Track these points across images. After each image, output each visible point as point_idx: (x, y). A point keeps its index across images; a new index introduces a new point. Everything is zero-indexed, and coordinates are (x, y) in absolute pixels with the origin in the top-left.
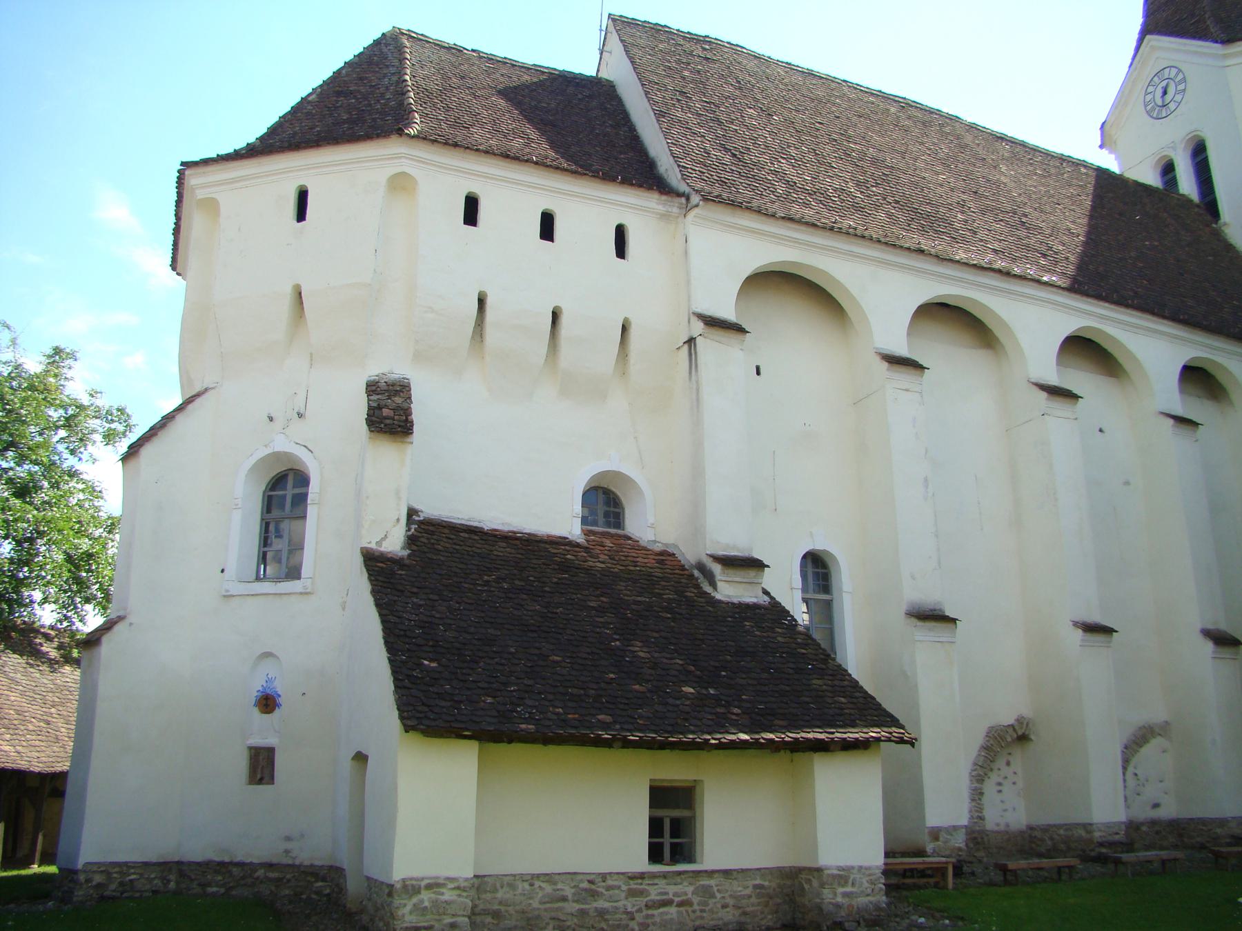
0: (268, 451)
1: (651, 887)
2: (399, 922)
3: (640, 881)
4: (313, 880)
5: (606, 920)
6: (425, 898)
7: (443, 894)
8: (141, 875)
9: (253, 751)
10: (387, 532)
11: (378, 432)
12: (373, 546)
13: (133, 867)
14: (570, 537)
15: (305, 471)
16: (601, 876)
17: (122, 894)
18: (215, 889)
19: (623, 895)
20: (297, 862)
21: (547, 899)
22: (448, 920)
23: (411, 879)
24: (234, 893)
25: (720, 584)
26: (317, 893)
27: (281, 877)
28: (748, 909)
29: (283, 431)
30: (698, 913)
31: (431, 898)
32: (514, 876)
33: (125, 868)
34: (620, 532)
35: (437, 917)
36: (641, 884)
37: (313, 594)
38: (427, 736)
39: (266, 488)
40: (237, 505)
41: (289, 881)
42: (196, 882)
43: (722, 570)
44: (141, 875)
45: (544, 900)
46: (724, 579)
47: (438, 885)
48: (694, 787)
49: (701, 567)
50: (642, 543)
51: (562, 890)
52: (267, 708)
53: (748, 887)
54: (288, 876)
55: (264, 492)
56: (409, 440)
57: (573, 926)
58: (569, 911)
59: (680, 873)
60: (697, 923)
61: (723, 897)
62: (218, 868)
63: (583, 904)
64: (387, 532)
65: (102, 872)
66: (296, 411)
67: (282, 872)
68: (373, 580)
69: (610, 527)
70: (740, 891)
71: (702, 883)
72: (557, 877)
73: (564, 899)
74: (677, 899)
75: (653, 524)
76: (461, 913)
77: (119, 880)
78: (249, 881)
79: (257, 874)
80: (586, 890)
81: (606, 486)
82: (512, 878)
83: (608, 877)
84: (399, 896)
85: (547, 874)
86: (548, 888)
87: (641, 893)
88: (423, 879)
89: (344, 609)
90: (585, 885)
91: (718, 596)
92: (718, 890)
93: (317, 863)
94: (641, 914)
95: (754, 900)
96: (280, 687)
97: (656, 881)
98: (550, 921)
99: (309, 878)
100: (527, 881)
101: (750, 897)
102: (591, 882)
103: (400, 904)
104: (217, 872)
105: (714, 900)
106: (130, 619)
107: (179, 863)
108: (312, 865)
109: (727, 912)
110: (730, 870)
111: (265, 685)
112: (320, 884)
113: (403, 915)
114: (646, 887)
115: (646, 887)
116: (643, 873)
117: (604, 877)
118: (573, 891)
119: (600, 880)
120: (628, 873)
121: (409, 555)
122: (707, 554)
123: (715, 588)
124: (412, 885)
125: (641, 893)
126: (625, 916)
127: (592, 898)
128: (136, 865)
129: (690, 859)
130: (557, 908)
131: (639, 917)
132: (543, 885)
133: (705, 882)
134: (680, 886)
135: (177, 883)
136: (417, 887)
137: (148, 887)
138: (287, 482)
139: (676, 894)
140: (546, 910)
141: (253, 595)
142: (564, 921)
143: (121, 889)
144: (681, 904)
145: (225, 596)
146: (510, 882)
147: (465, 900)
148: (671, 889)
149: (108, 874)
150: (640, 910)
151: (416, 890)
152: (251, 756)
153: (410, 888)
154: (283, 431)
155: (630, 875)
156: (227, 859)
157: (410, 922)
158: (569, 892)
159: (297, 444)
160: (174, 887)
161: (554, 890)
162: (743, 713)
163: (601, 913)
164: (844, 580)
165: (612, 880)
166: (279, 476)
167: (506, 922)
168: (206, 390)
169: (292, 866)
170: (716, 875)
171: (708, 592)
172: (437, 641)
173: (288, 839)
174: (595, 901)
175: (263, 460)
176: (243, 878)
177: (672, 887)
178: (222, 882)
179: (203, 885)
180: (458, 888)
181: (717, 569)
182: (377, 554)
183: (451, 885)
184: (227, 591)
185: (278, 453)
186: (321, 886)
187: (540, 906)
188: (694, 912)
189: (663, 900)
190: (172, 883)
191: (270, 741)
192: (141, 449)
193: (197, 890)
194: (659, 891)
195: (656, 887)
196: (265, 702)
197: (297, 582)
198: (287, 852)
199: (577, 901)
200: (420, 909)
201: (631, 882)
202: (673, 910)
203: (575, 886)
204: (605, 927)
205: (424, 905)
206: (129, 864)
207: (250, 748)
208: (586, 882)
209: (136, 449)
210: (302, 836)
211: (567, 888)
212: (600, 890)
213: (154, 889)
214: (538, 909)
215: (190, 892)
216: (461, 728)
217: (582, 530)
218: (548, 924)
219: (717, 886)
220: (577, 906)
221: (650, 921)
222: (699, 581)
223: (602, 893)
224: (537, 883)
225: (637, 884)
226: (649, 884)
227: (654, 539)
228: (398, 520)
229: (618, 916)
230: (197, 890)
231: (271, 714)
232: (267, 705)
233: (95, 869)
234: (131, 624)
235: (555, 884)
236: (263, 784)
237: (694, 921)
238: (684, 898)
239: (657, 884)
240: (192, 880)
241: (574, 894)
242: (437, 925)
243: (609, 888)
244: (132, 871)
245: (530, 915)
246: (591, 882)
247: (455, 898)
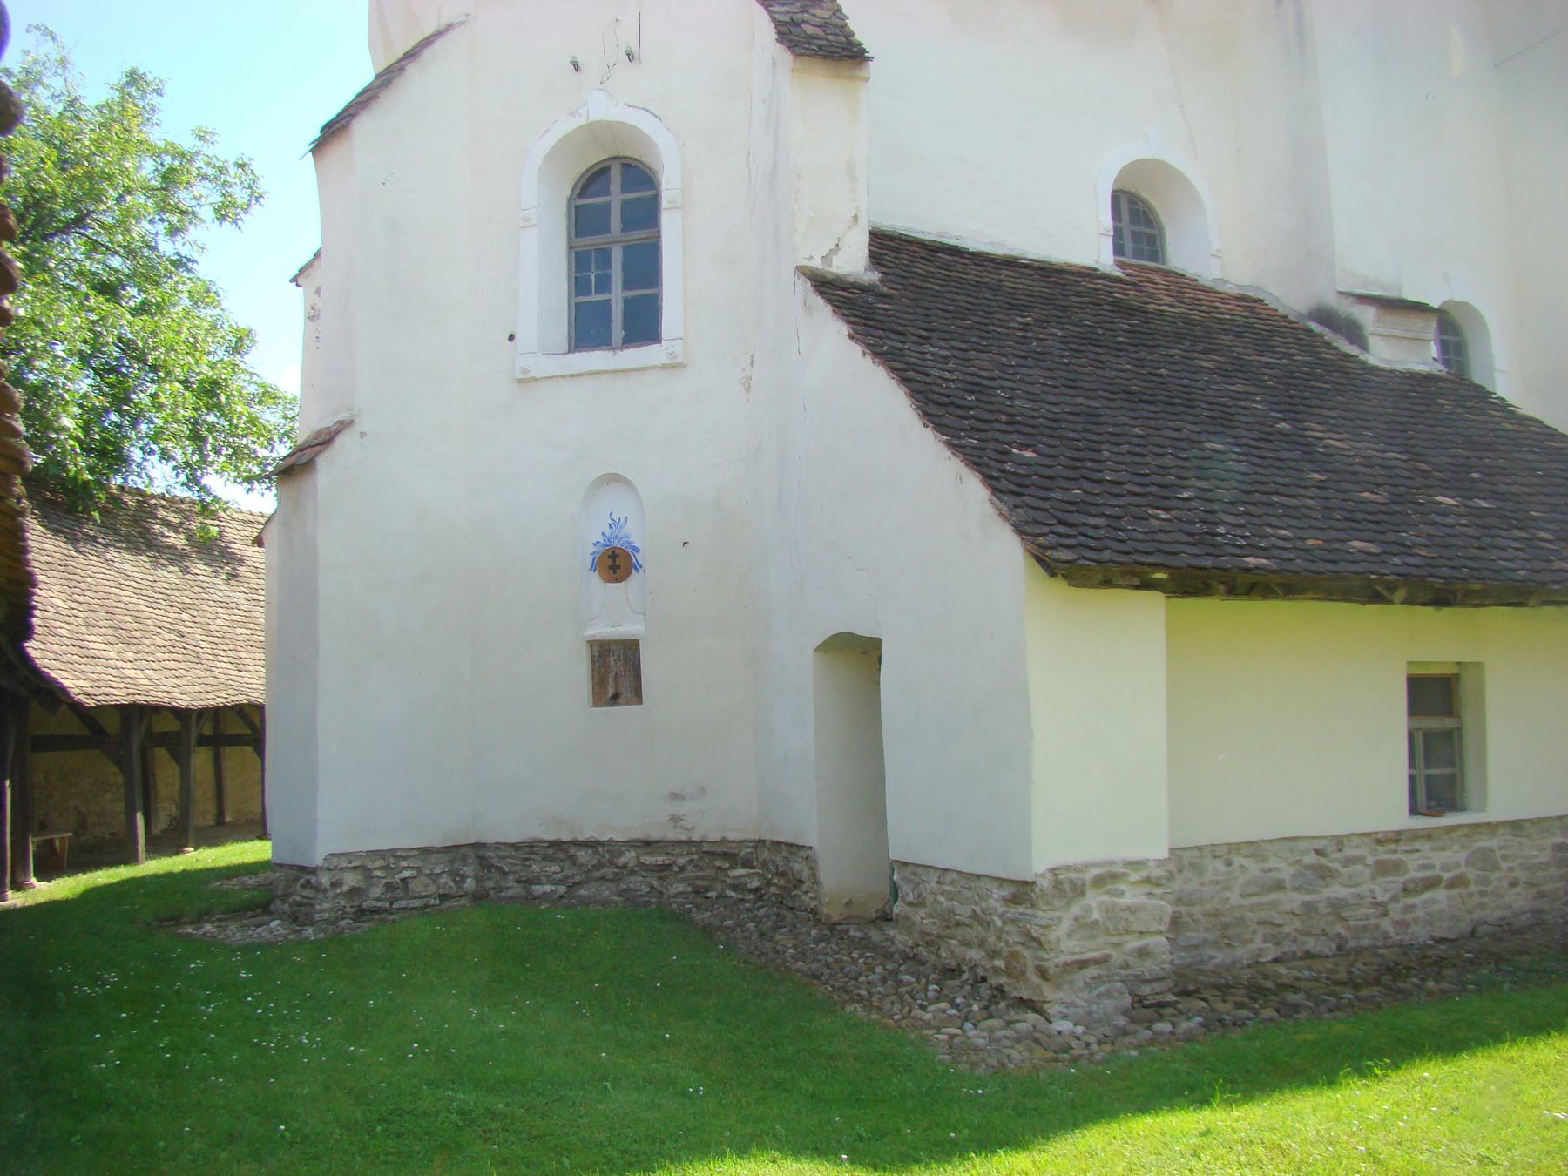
0: (581, 121)
1: (1410, 855)
2: (1052, 955)
3: (1392, 847)
4: (728, 865)
5: (1343, 919)
6: (1093, 905)
7: (1122, 893)
8: (419, 869)
9: (596, 648)
10: (839, 239)
11: (810, 56)
12: (817, 264)
13: (405, 858)
14: (1100, 268)
15: (643, 159)
16: (1335, 841)
17: (391, 903)
18: (548, 888)
19: (1368, 872)
20: (696, 837)
21: (1252, 889)
22: (1133, 943)
23: (1068, 868)
24: (582, 892)
25: (1373, 342)
26: (734, 887)
27: (667, 862)
28: (1548, 887)
29: (601, 87)
30: (1477, 899)
31: (1103, 902)
32: (1200, 848)
33: (392, 860)
34: (1161, 266)
35: (1115, 939)
36: (1395, 851)
37: (685, 366)
38: (1076, 586)
39: (572, 194)
40: (527, 220)
41: (682, 869)
42: (511, 878)
43: (1376, 315)
44: (419, 869)
45: (1248, 891)
46: (1380, 331)
47: (1114, 877)
48: (1457, 677)
49: (1326, 317)
50: (1202, 282)
51: (1277, 869)
52: (615, 572)
53: (1545, 849)
54: (681, 861)
55: (569, 200)
56: (863, 74)
57: (1294, 934)
58: (1288, 907)
59: (1450, 829)
60: (1477, 915)
61: (1511, 869)
62: (551, 851)
63: (1309, 892)
64: (839, 239)
65: (355, 868)
66: (623, 49)
67: (667, 854)
68: (847, 316)
69: (1143, 259)
70: (1536, 856)
71: (1478, 844)
72: (1267, 846)
73: (1279, 886)
74: (1446, 876)
75: (1219, 251)
76: (1154, 927)
77: (385, 880)
78: (609, 871)
79: (622, 860)
80: (1311, 867)
81: (1133, 190)
82: (1196, 853)
83: (1346, 842)
84: (1048, 904)
85: (1251, 843)
86: (1254, 868)
87: (1397, 867)
88: (1087, 866)
89: (748, 389)
90: (1310, 859)
91: (1372, 361)
92: (1504, 857)
93: (732, 836)
94: (1398, 906)
95: (1553, 871)
96: (634, 534)
97: (1417, 845)
98: (1259, 928)
99: (718, 863)
100: (1220, 857)
101: (1548, 864)
102: (1319, 853)
103: (1051, 919)
104: (546, 858)
105: (1497, 874)
106: (363, 424)
107: (478, 846)
108: (724, 841)
109: (1518, 894)
110: (1523, 820)
111: (608, 532)
112: (740, 871)
113: (1058, 941)
114: (1403, 857)
115: (1403, 857)
116: (1399, 833)
117: (1340, 841)
118: (1291, 870)
119: (1335, 848)
120: (1377, 833)
121: (881, 281)
122: (1341, 293)
123: (1363, 345)
124: (1071, 881)
125: (1397, 867)
126: (1373, 910)
127: (1321, 882)
128: (411, 854)
129: (1455, 806)
130: (1270, 904)
131: (1395, 911)
132: (1246, 862)
133: (1485, 842)
134: (1448, 853)
135: (478, 879)
136: (1080, 883)
137: (432, 889)
138: (608, 181)
139: (1445, 868)
140: (1251, 908)
141: (572, 376)
142: (1279, 926)
143: (389, 895)
144: (1452, 884)
145: (520, 381)
146: (1192, 861)
147: (1162, 903)
148: (1439, 858)
149: (366, 870)
150: (1394, 899)
151: (1079, 891)
152: (593, 657)
153: (1067, 886)
154: (601, 87)
155: (1380, 836)
156: (566, 837)
157: (1071, 953)
158: (1286, 872)
159: (630, 106)
160: (474, 886)
161: (1264, 871)
162: (1557, 539)
163: (1337, 906)
164: (1495, 351)
165: (1352, 847)
166: (596, 169)
167: (1190, 934)
168: (450, 27)
169: (690, 843)
170: (1501, 830)
171: (1353, 354)
172: (1012, 415)
173: (676, 796)
174: (1327, 886)
175: (566, 140)
176: (595, 868)
177: (1439, 853)
178: (559, 876)
179: (527, 882)
180: (1147, 880)
181: (1367, 316)
182: (829, 277)
183: (1134, 877)
184: (525, 371)
185: (599, 123)
186: (742, 876)
187: (1244, 902)
188: (1470, 896)
189: (1427, 879)
190: (469, 880)
191: (628, 628)
192: (353, 122)
193: (518, 890)
194: (1421, 862)
195: (1417, 855)
196: (610, 562)
197: (655, 347)
198: (675, 819)
199: (1297, 889)
200: (1084, 925)
201: (1380, 848)
202: (1440, 894)
203: (1298, 862)
204: (1343, 932)
205: (1091, 919)
206: (399, 853)
207: (591, 644)
208: (1313, 854)
209: (344, 122)
210: (703, 790)
211: (1282, 866)
212: (1334, 865)
213: (441, 891)
214: (1240, 906)
215: (503, 894)
216: (1150, 565)
217: (1115, 261)
218: (1254, 932)
219: (1501, 848)
220: (1301, 897)
221: (1408, 917)
222: (1326, 338)
223: (1337, 871)
224: (1238, 860)
225: (1388, 852)
226: (1407, 851)
227: (1220, 276)
228: (855, 218)
229: (1363, 911)
230: (518, 890)
232: (614, 568)
233: (344, 864)
234: (363, 434)
235: (1265, 860)
236: (619, 705)
237: (1470, 912)
238: (1457, 872)
239: (1418, 851)
240: (504, 873)
241: (1294, 876)
242: (1113, 952)
243: (1349, 861)
244: (405, 864)
245: (1226, 919)
246: (1319, 853)
247: (1143, 899)
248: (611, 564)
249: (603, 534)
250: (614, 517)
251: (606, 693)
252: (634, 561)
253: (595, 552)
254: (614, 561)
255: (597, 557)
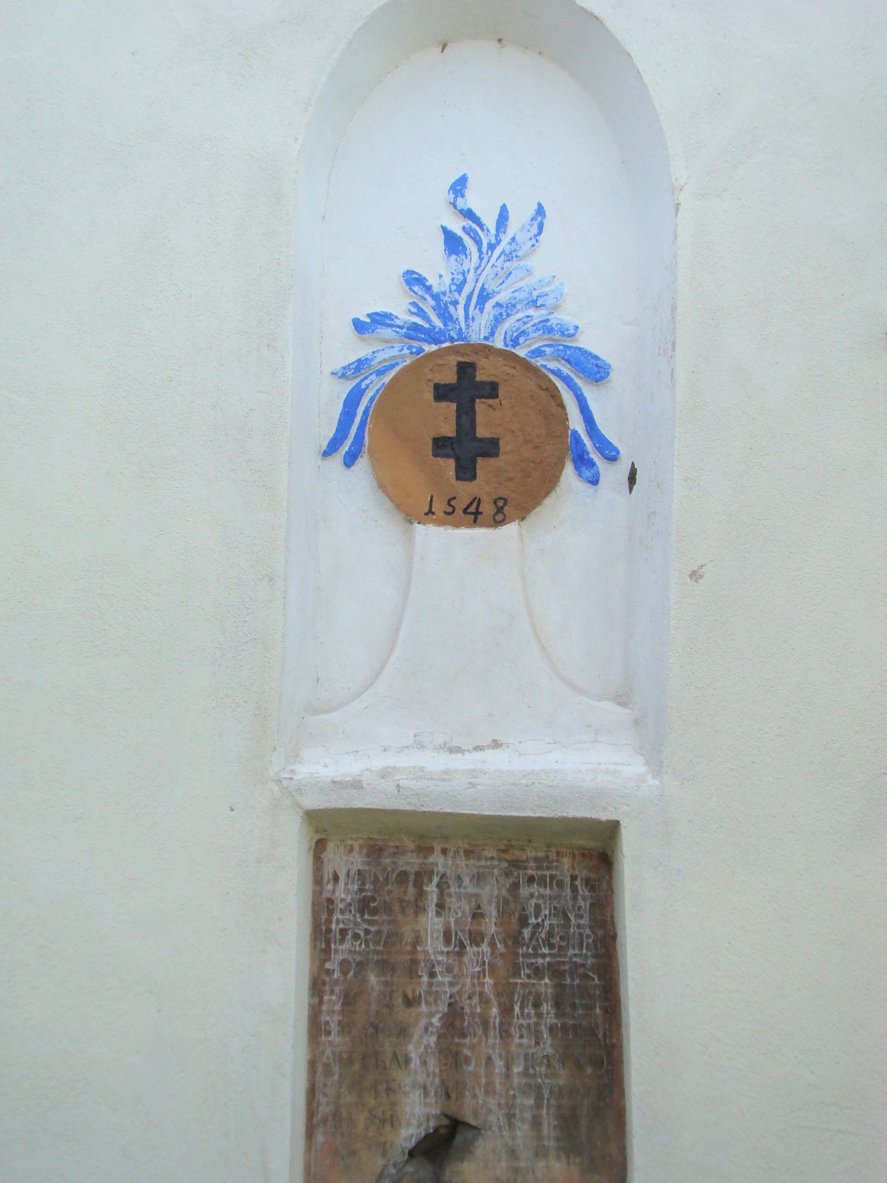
52: (466, 472)
231: (511, 529)
248: (449, 430)
249: (413, 279)
250: (472, 200)
251: (391, 1120)
252: (576, 422)
253: (361, 365)
254: (466, 415)
255: (375, 386)
